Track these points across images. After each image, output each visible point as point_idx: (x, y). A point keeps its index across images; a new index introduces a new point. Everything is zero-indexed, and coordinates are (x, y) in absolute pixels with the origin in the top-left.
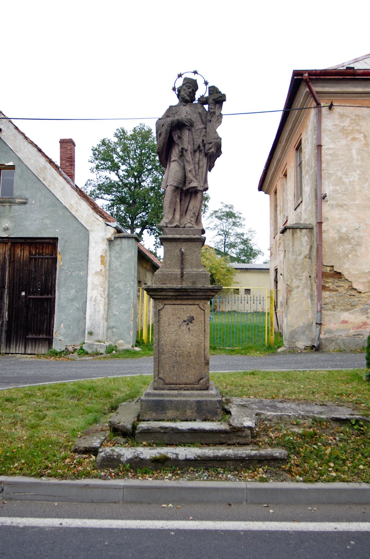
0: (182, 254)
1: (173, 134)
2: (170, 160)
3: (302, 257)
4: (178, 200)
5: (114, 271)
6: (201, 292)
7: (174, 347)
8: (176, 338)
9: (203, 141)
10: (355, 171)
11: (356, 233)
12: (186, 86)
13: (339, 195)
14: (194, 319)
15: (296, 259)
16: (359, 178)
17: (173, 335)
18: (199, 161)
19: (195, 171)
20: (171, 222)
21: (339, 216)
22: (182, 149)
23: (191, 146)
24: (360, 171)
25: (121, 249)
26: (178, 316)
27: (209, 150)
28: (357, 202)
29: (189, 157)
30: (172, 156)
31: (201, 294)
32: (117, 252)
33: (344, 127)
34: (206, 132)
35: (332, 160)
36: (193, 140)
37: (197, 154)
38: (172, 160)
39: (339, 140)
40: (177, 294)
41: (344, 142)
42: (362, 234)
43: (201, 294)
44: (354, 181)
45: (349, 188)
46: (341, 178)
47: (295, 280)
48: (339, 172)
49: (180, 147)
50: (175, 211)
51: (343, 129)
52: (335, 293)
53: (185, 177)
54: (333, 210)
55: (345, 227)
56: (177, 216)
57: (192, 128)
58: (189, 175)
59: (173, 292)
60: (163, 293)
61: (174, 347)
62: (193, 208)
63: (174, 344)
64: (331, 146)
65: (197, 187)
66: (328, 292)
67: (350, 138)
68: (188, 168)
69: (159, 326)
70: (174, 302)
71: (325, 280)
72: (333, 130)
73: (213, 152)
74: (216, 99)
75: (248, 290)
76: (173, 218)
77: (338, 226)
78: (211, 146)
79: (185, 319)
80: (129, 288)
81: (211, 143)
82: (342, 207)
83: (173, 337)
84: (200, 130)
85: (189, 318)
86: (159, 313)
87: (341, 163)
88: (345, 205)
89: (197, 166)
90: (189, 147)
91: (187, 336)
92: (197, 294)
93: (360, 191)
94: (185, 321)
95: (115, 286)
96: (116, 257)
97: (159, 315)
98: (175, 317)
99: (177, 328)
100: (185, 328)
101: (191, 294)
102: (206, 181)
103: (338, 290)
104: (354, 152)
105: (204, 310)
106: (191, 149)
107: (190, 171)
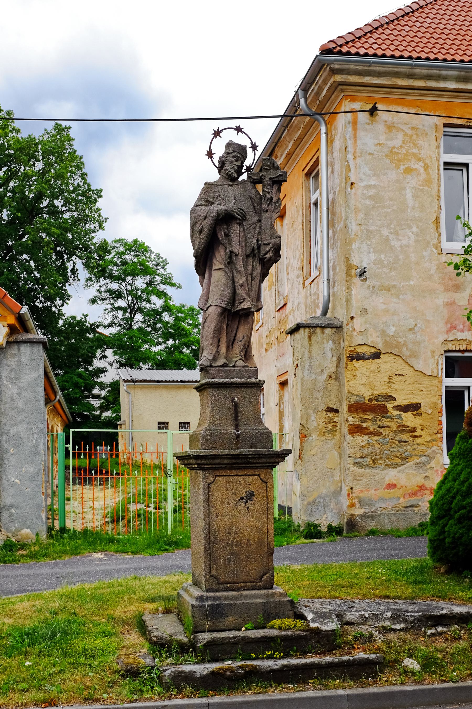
0: (236, 406)
1: (218, 229)
2: (212, 267)
3: (325, 376)
4: (225, 327)
5: (8, 405)
6: (264, 458)
7: (230, 533)
8: (232, 522)
9: (258, 240)
10: (410, 227)
11: (411, 336)
12: (233, 157)
13: (385, 270)
14: (254, 495)
15: (316, 380)
16: (417, 241)
17: (228, 517)
18: (252, 270)
19: (248, 284)
20: (215, 359)
21: (384, 307)
22: (231, 252)
23: (242, 248)
24: (418, 227)
25: (19, 363)
26: (233, 491)
27: (265, 254)
28: (412, 283)
29: (240, 264)
30: (215, 261)
31: (264, 460)
32: (12, 370)
33: (394, 148)
34: (260, 227)
35: (373, 207)
36: (246, 240)
37: (250, 260)
38: (214, 267)
39: (386, 171)
40: (233, 461)
41: (393, 175)
42: (419, 338)
43: (264, 460)
44: (408, 246)
45: (401, 257)
46: (387, 239)
47: (313, 418)
48: (385, 228)
49: (228, 251)
50: (219, 341)
51: (391, 152)
52: (376, 438)
53: (234, 293)
54: (374, 296)
55: (393, 326)
56: (223, 350)
57: (244, 223)
58: (241, 292)
59: (229, 458)
60: (216, 461)
61: (230, 533)
62: (244, 337)
63: (229, 529)
64: (373, 183)
65: (250, 308)
66: (366, 437)
67: (402, 167)
68: (241, 280)
69: (209, 506)
70: (229, 472)
71: (362, 416)
72: (375, 153)
73: (271, 257)
74: (274, 178)
75: (185, 423)
76: (218, 352)
77: (383, 323)
78: (268, 249)
79: (243, 495)
80: (36, 436)
81: (268, 244)
82: (389, 290)
83: (229, 521)
84: (254, 226)
85: (248, 494)
86: (209, 488)
87: (387, 212)
88: (394, 286)
89: (250, 279)
90: (241, 250)
91: (246, 518)
92: (260, 461)
93: (417, 263)
94: (242, 498)
95: (11, 432)
96: (10, 378)
97: (209, 491)
98: (230, 493)
99: (232, 508)
100: (242, 508)
101: (252, 460)
102: (258, 299)
103: (381, 433)
104: (409, 194)
105: (267, 483)
106: (242, 252)
107: (242, 285)
